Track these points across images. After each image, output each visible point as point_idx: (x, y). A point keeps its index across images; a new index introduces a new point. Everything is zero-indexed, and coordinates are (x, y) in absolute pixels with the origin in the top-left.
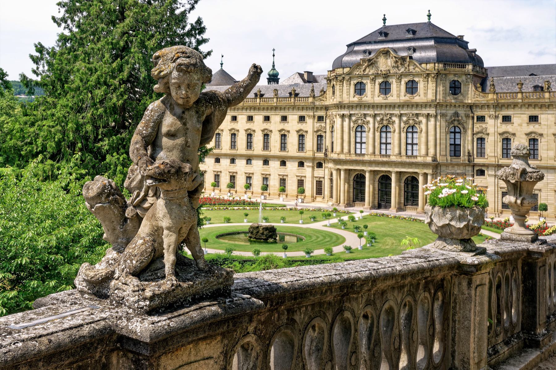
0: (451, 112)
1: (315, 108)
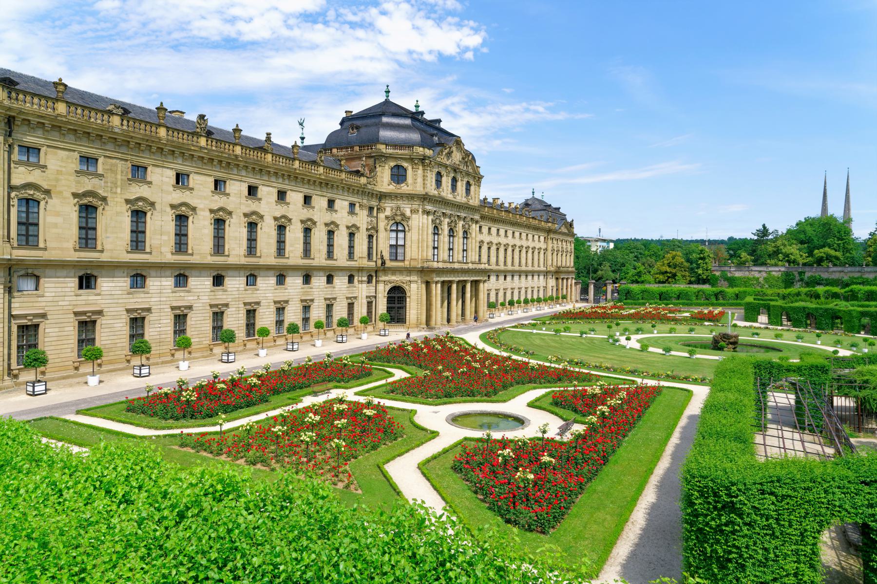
1: (371, 195)
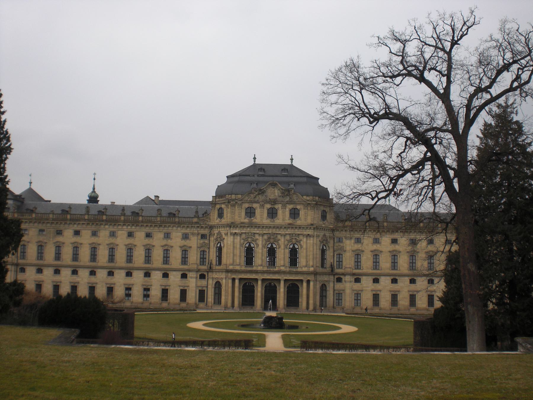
0: (322, 234)
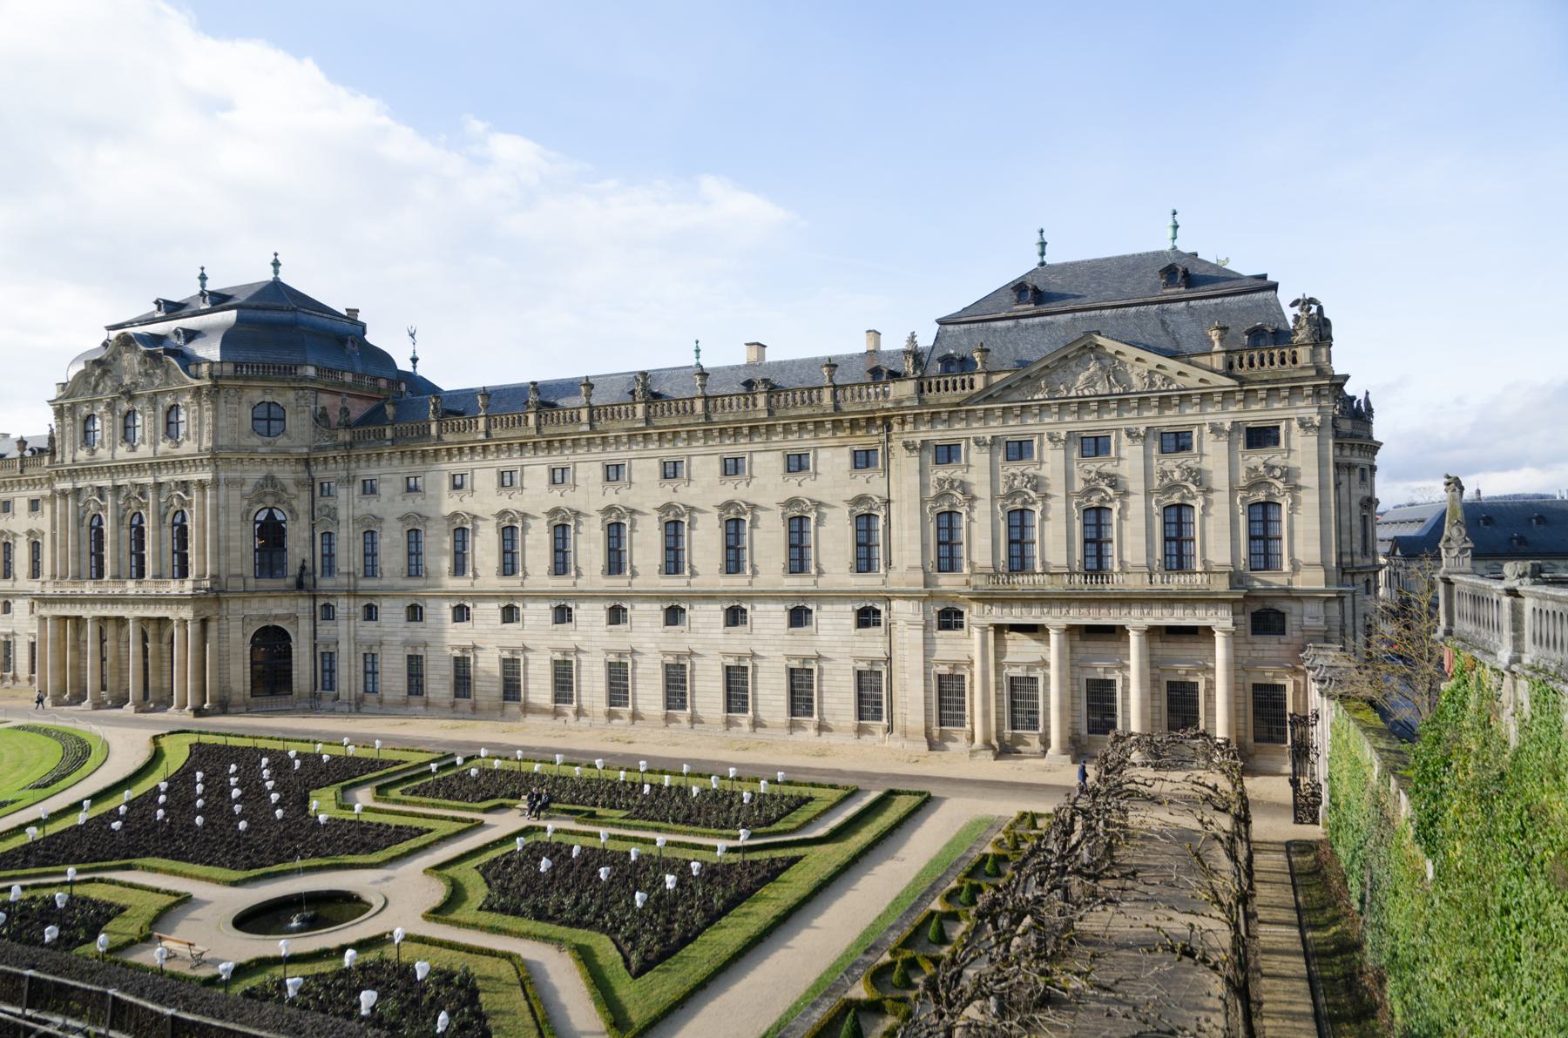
0: (254, 474)
